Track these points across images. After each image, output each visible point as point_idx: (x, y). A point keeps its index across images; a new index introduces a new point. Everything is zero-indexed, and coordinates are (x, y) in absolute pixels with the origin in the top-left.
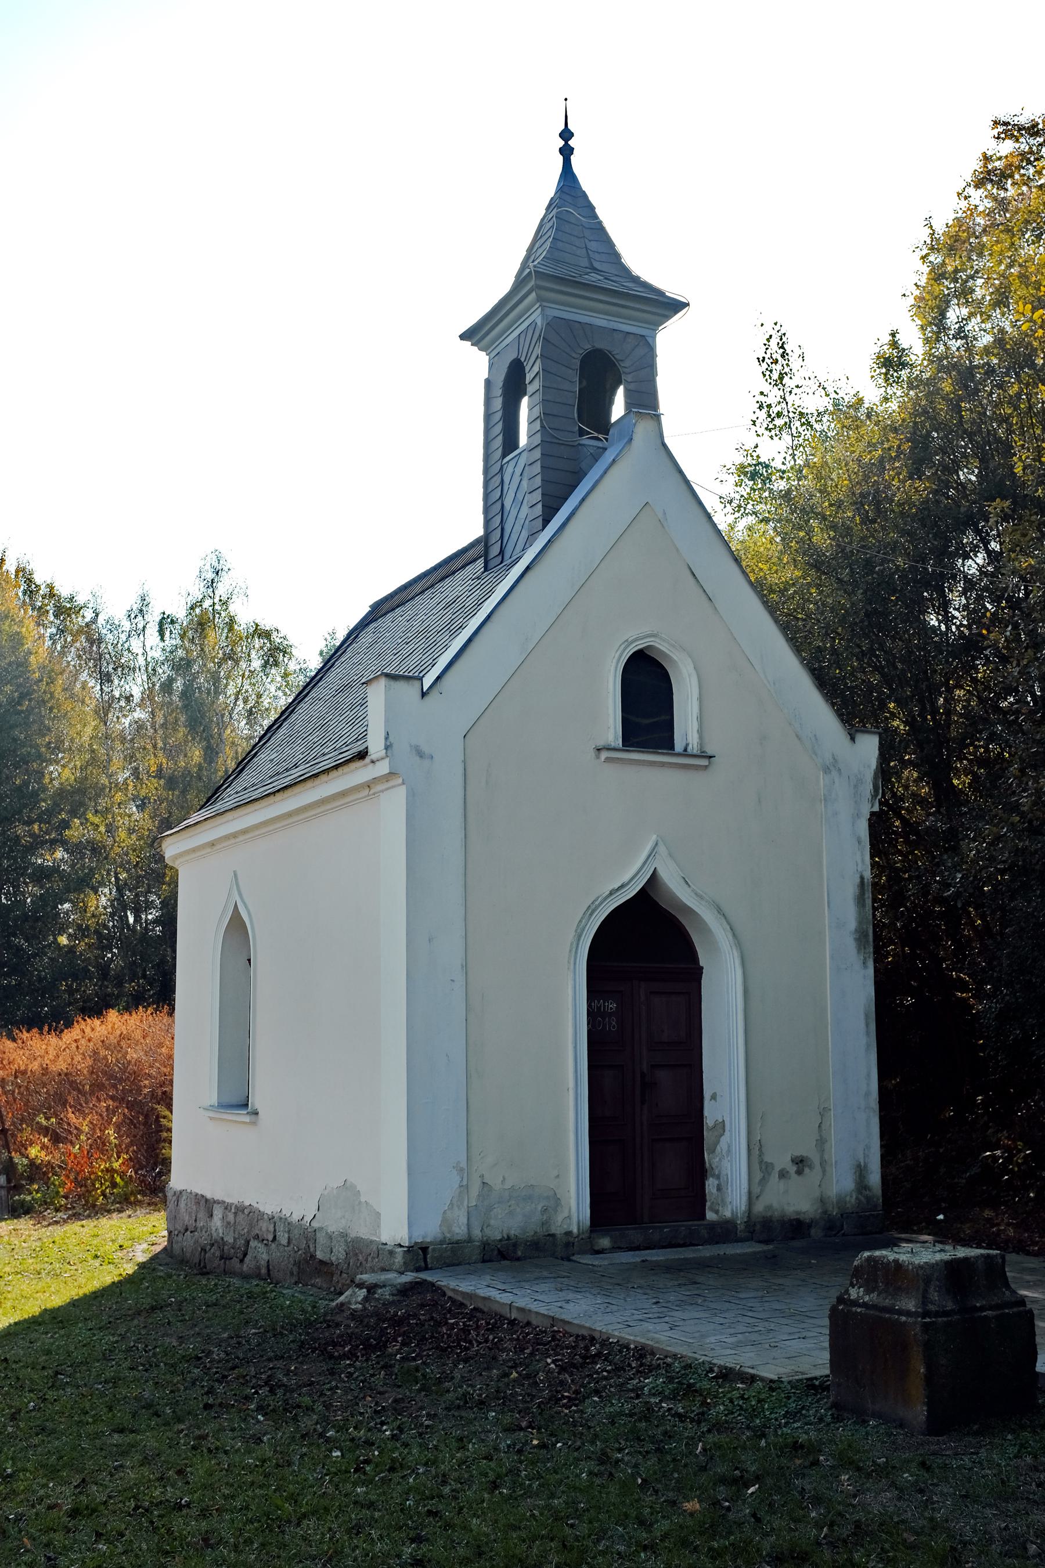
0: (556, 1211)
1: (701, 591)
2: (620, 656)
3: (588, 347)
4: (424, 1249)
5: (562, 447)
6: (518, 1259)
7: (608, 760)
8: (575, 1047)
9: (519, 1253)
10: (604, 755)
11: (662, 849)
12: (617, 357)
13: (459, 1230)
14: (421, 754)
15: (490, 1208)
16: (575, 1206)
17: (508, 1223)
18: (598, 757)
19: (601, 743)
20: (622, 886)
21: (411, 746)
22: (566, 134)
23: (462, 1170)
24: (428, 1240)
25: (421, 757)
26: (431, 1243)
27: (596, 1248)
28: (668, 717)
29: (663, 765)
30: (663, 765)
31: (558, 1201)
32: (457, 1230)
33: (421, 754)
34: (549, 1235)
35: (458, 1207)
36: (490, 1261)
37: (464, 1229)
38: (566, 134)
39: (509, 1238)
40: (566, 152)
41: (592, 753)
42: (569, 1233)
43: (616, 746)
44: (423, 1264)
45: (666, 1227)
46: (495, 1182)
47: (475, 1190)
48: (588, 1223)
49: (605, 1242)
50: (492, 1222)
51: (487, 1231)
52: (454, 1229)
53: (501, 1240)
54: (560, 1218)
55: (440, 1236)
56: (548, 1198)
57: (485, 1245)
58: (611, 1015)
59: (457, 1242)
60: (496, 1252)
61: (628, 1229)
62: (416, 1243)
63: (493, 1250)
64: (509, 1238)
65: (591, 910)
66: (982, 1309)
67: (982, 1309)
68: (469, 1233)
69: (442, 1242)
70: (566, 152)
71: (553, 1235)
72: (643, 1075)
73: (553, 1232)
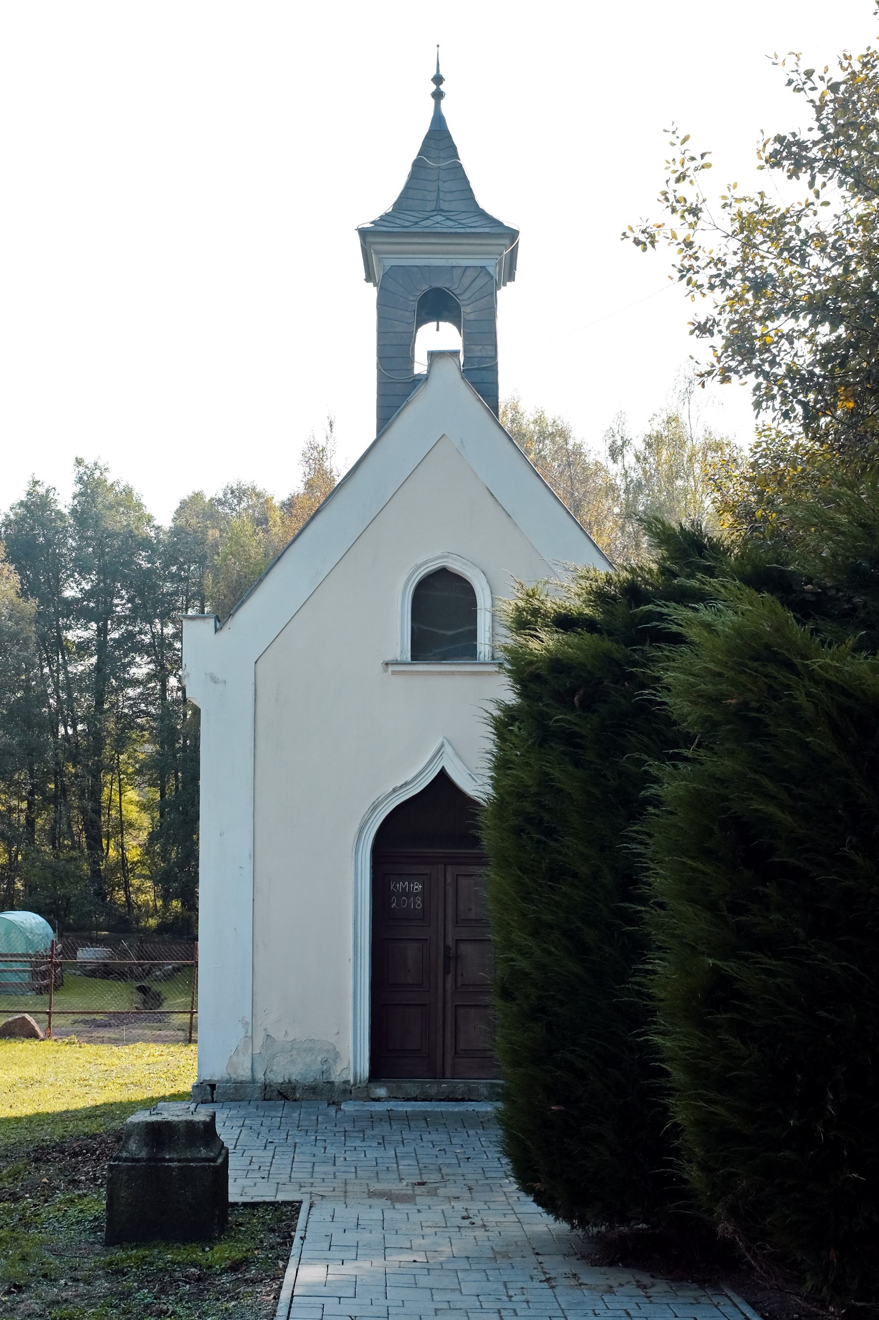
0: (335, 1062)
1: (501, 509)
2: (409, 579)
3: (425, 287)
4: (213, 1087)
5: (398, 385)
6: (295, 1100)
7: (394, 673)
8: (355, 924)
9: (298, 1095)
10: (391, 668)
11: (448, 749)
12: (455, 292)
13: (244, 1073)
14: (215, 680)
15: (274, 1056)
16: (353, 1057)
17: (283, 1071)
18: (386, 671)
19: (389, 658)
20: (406, 784)
21: (206, 674)
22: (438, 80)
23: (247, 1023)
24: (216, 1078)
25: (215, 682)
26: (218, 1081)
27: (372, 1096)
28: (472, 628)
29: (453, 673)
30: (453, 673)
31: (337, 1055)
32: (242, 1073)
33: (215, 680)
34: (328, 1082)
35: (244, 1054)
36: (270, 1100)
37: (250, 1073)
38: (438, 80)
39: (290, 1082)
40: (438, 96)
41: (380, 667)
42: (347, 1082)
43: (404, 658)
44: (210, 1098)
45: (444, 1083)
46: (278, 1035)
47: (259, 1040)
48: (366, 1074)
49: (382, 1092)
50: (275, 1068)
51: (270, 1076)
52: (239, 1071)
53: (282, 1084)
54: (339, 1068)
55: (226, 1077)
56: (328, 1051)
57: (266, 1086)
58: (416, 895)
59: (241, 1082)
60: (276, 1093)
61: (404, 1082)
62: (205, 1081)
63: (273, 1091)
64: (290, 1082)
65: (375, 807)
66: (170, 1160)
67: (170, 1160)
68: (253, 1076)
69: (228, 1081)
70: (438, 96)
71: (332, 1083)
72: (447, 948)
73: (333, 1079)
